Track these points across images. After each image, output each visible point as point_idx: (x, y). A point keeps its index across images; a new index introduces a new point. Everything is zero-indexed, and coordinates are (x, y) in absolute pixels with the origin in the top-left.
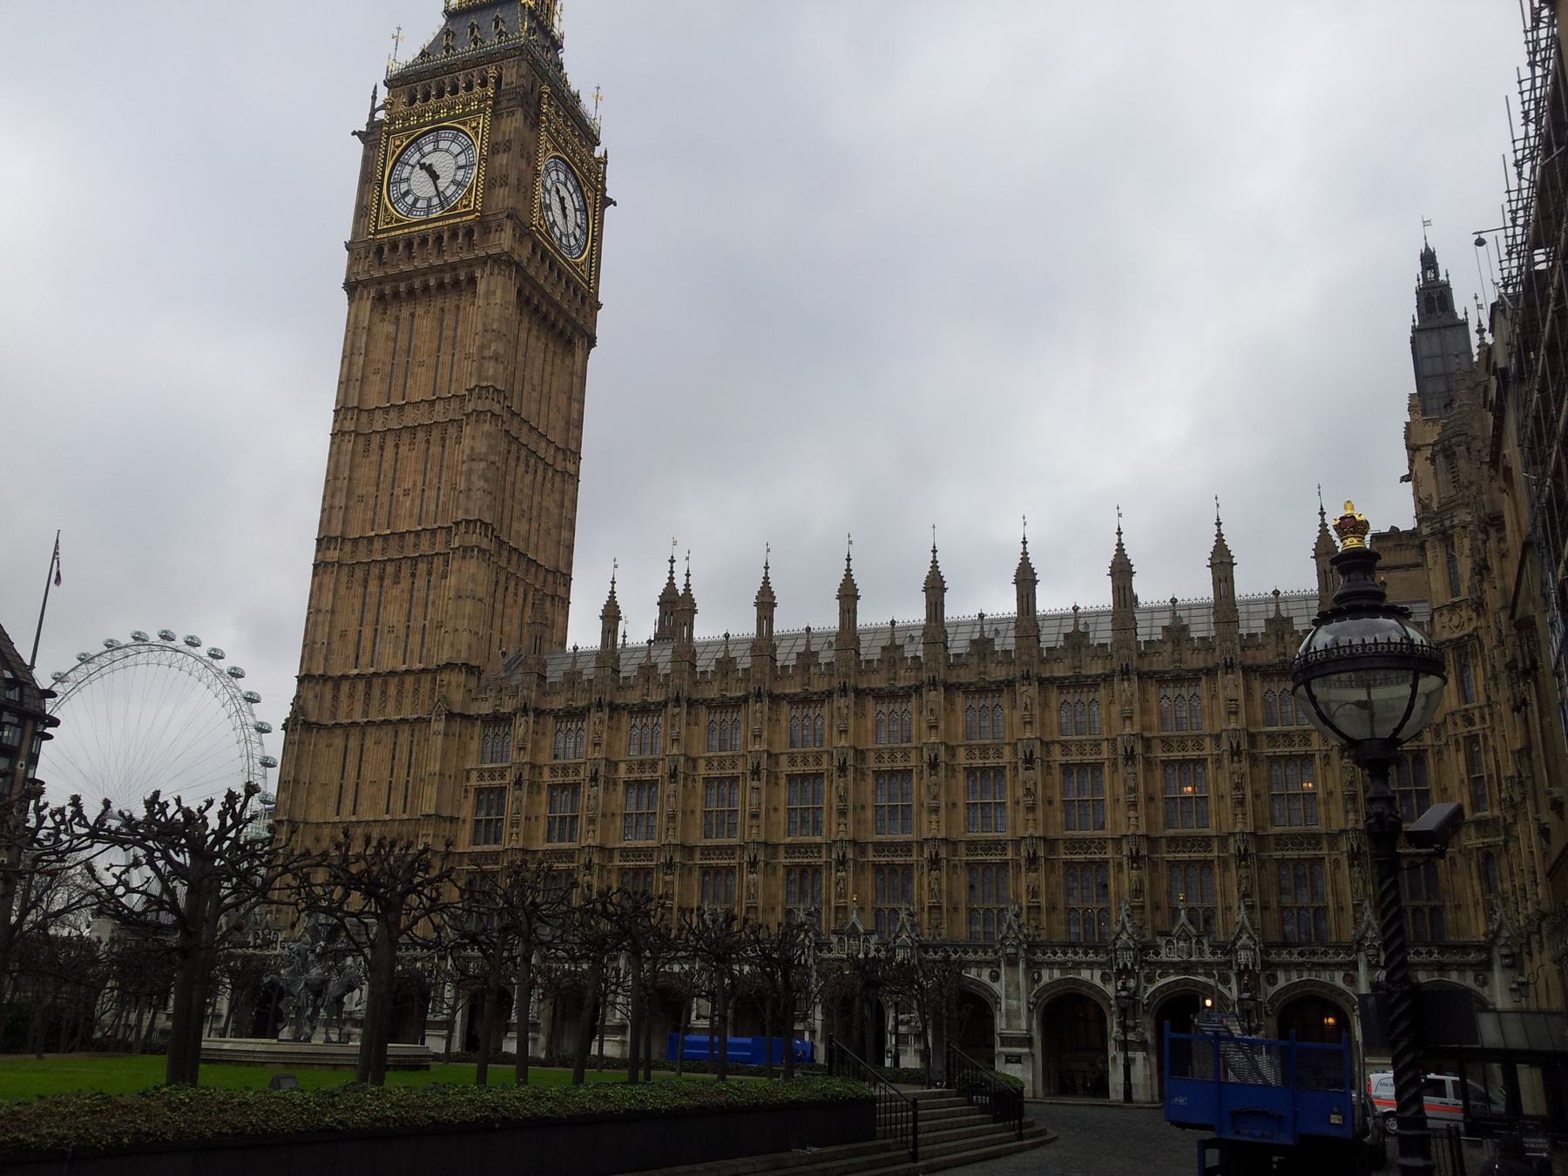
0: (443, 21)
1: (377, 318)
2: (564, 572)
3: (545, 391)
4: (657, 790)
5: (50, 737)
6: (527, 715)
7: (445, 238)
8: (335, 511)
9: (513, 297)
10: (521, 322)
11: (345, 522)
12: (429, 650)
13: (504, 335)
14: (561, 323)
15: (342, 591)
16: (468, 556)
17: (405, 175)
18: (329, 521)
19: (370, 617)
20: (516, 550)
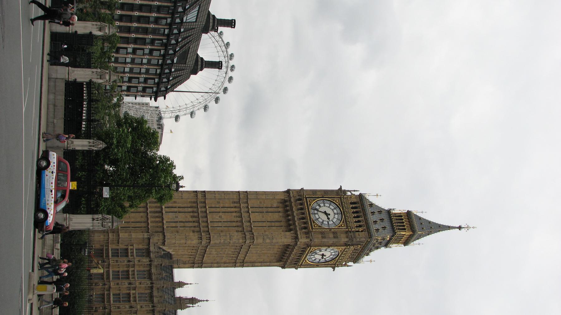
1: (279, 201)
2: (203, 266)
7: (303, 220)
8: (214, 195)
11: (211, 199)
14: (286, 258)
17: (326, 205)
19: (181, 210)
20: (206, 251)
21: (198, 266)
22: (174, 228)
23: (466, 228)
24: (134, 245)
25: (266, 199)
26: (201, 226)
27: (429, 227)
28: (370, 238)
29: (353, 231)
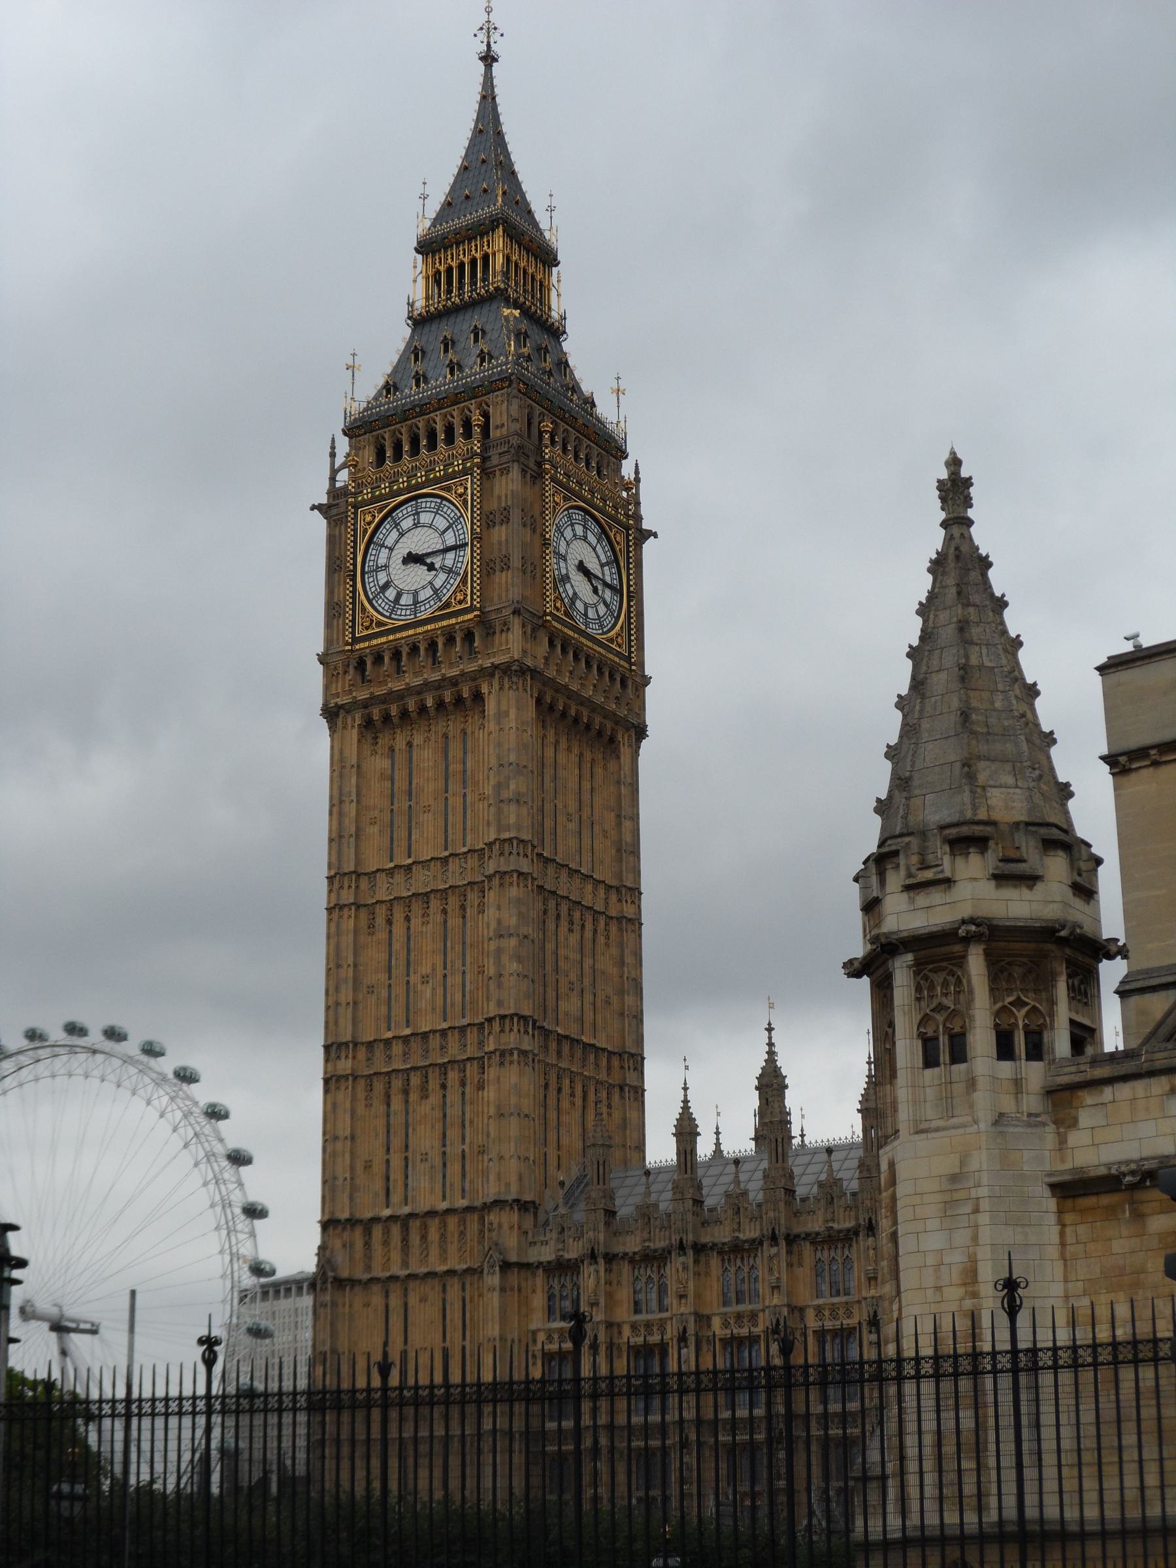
0: (408, 331)
1: (367, 748)
2: (633, 1051)
3: (584, 817)
4: (760, 1348)
5: (18, 1282)
6: (596, 1263)
8: (341, 1010)
9: (531, 712)
10: (544, 737)
12: (471, 1182)
13: (525, 767)
14: (598, 720)
15: (361, 1110)
16: (507, 1063)
17: (382, 561)
18: (336, 1023)
19: (397, 1142)
20: (567, 1037)
21: (635, 1069)
22: (468, 1168)
23: (489, 37)
24: (533, 1327)
25: (358, 801)
26: (459, 1058)
27: (484, 167)
28: (511, 382)
29: (485, 448)
